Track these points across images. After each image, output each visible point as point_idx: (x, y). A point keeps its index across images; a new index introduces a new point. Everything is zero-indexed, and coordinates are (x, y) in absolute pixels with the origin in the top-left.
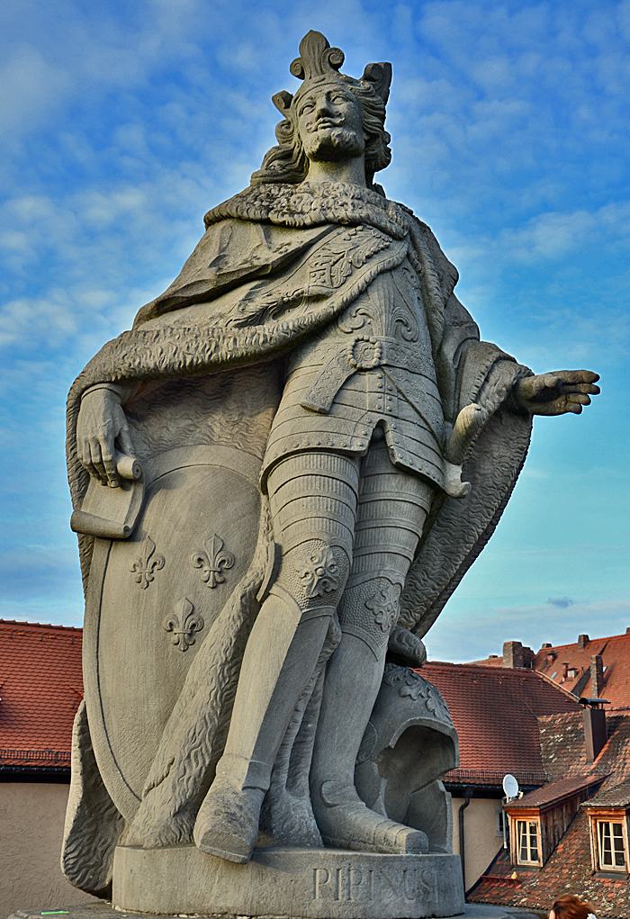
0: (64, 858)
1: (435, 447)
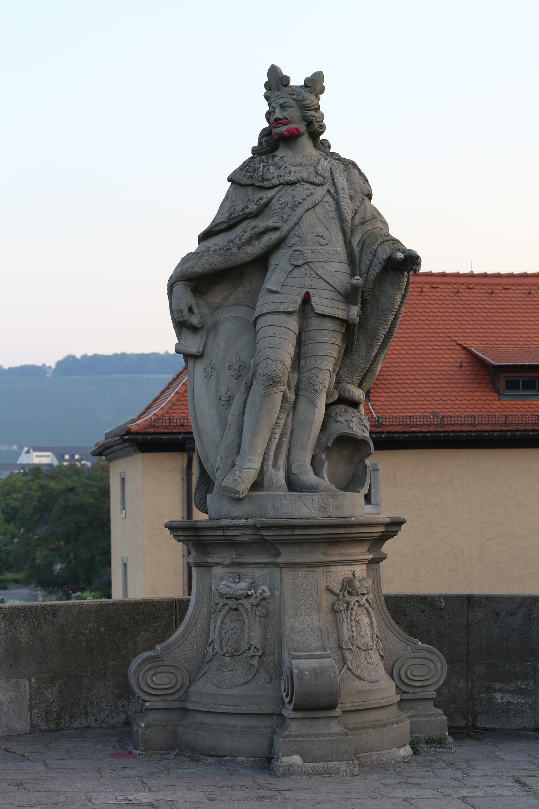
0: (194, 500)
1: (341, 298)
